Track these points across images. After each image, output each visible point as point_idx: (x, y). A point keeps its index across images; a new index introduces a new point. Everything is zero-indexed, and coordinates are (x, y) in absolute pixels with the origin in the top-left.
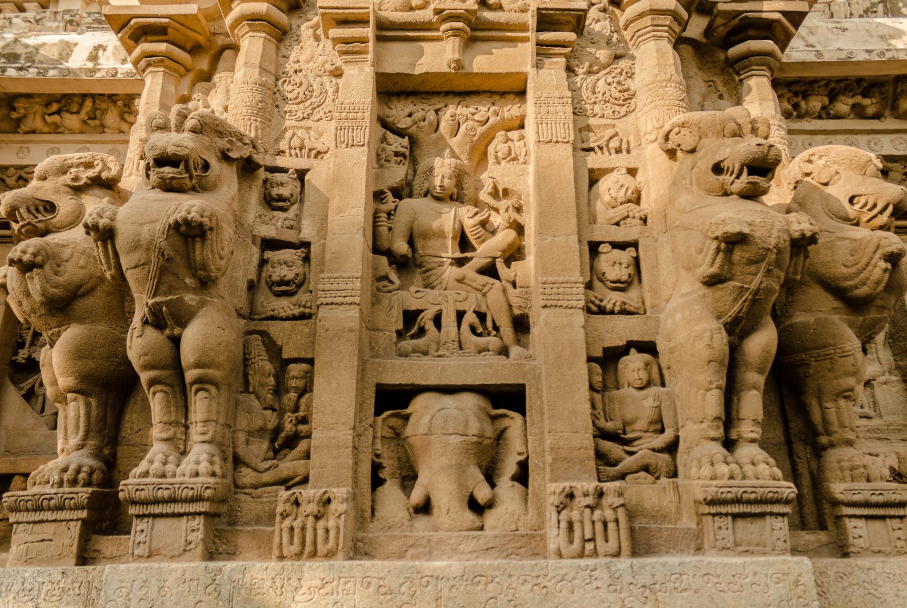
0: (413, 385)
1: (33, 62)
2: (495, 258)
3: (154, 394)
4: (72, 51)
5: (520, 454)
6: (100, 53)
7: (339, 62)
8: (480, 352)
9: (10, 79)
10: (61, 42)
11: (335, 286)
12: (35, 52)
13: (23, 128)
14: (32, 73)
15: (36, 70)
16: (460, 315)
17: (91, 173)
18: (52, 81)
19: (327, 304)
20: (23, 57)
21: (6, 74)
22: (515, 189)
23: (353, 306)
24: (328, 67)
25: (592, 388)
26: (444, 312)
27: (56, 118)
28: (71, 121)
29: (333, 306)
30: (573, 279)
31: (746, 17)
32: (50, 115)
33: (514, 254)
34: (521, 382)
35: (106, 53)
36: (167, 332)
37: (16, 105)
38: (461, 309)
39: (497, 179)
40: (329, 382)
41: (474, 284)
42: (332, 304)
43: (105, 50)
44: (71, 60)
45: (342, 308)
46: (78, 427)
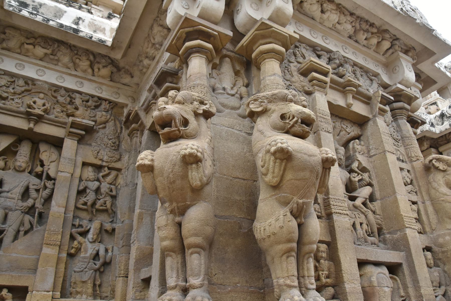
0: (367, 260)
1: (38, 12)
2: (366, 199)
3: (288, 257)
4: (63, 15)
5: (402, 297)
6: (80, 22)
7: (311, 89)
8: (372, 244)
9: (24, 17)
10: (56, 6)
11: (337, 204)
12: (39, 7)
13: (4, 45)
14: (39, 18)
15: (42, 18)
16: (361, 224)
17: (204, 107)
18: (51, 27)
19: (336, 213)
20: (31, 7)
21: (21, 13)
22: (368, 168)
23: (346, 216)
24: (306, 88)
25: (429, 266)
26: (356, 222)
27: (31, 47)
28: (40, 51)
29: (339, 215)
30: (409, 215)
31: (413, 119)
32: (27, 44)
33: (372, 198)
34: (401, 262)
35: (84, 23)
36: (299, 220)
37: (7, 31)
38: (362, 222)
39: (361, 161)
40: (346, 257)
41: (362, 210)
42: (339, 213)
43: (83, 21)
44: (62, 19)
45: (343, 216)
46: (200, 271)
